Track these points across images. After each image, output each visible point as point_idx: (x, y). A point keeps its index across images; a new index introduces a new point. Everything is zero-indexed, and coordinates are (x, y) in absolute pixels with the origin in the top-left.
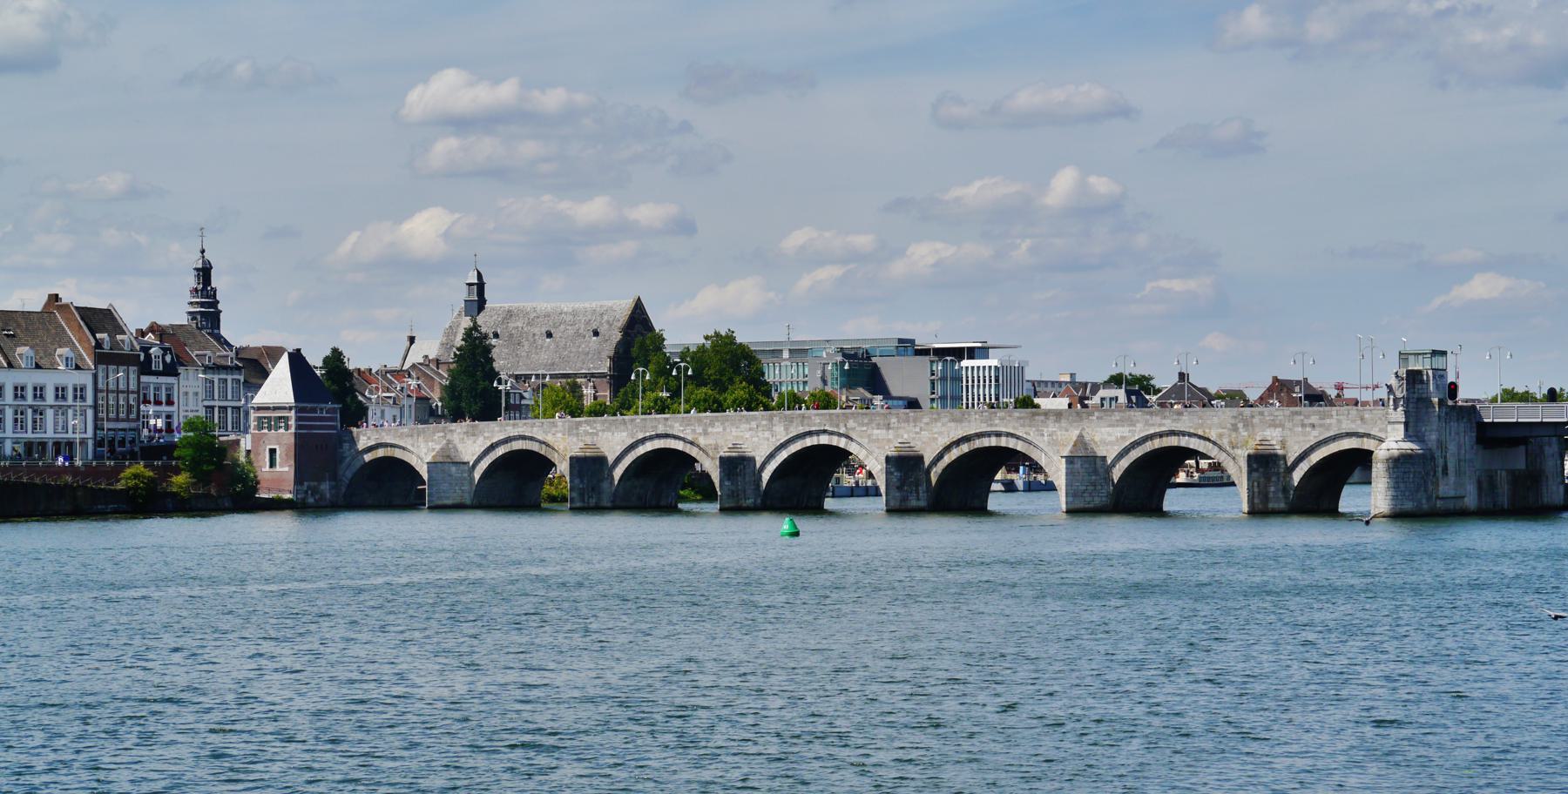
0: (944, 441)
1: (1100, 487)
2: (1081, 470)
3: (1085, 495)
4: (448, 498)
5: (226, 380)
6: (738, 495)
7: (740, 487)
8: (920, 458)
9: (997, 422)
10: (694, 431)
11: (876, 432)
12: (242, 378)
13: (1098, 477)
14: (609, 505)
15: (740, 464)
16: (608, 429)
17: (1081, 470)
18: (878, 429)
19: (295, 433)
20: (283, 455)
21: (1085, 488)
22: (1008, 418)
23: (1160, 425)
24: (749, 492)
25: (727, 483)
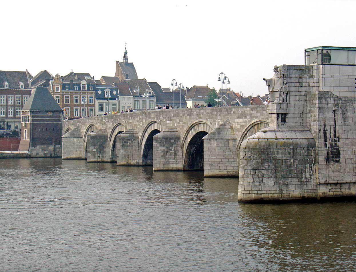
0: (186, 128)
1: (232, 160)
2: (216, 148)
3: (220, 165)
4: (73, 154)
5: (139, 101)
6: (128, 157)
7: (129, 153)
8: (179, 138)
9: (201, 115)
10: (126, 121)
11: (168, 122)
12: (155, 101)
13: (231, 153)
14: (109, 160)
15: (130, 140)
16: (108, 122)
17: (216, 148)
18: (168, 120)
19: (30, 123)
20: (28, 134)
21: (220, 160)
22: (205, 113)
23: (256, 117)
24: (135, 156)
25: (121, 151)
